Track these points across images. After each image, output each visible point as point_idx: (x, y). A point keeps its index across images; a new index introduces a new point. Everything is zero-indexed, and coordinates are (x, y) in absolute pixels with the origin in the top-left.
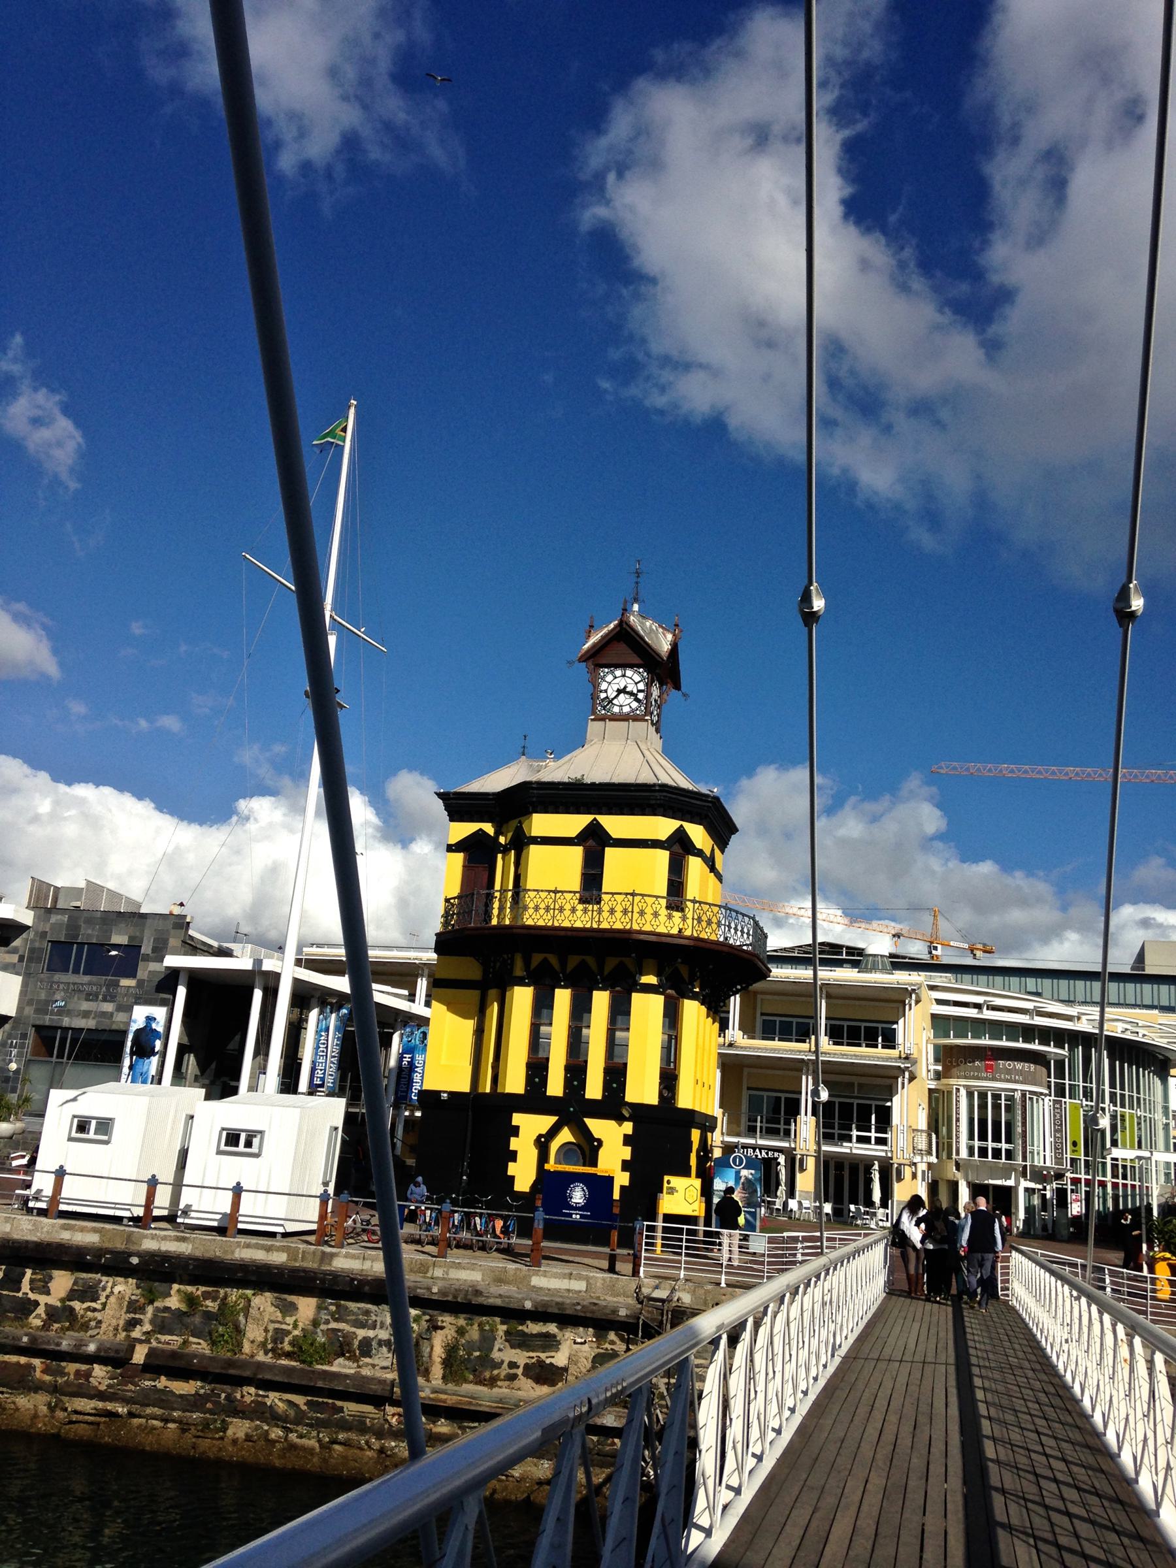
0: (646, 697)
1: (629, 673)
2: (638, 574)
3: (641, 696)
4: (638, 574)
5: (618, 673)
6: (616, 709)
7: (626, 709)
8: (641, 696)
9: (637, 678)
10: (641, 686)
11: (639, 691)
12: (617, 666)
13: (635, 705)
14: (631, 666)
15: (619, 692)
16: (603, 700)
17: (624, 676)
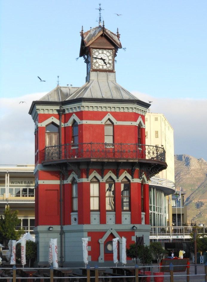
0: (113, 63)
1: (105, 52)
2: (100, 9)
3: (110, 62)
4: (100, 9)
5: (100, 51)
6: (101, 67)
7: (105, 67)
8: (110, 62)
9: (108, 54)
10: (110, 58)
11: (109, 60)
12: (100, 49)
13: (108, 65)
14: (105, 49)
15: (101, 59)
16: (95, 63)
17: (103, 53)
